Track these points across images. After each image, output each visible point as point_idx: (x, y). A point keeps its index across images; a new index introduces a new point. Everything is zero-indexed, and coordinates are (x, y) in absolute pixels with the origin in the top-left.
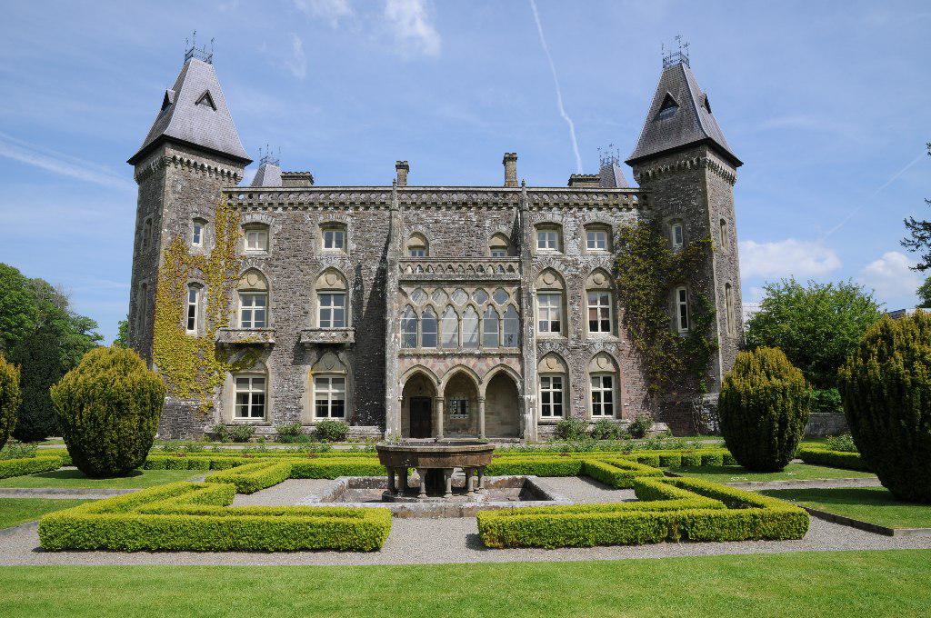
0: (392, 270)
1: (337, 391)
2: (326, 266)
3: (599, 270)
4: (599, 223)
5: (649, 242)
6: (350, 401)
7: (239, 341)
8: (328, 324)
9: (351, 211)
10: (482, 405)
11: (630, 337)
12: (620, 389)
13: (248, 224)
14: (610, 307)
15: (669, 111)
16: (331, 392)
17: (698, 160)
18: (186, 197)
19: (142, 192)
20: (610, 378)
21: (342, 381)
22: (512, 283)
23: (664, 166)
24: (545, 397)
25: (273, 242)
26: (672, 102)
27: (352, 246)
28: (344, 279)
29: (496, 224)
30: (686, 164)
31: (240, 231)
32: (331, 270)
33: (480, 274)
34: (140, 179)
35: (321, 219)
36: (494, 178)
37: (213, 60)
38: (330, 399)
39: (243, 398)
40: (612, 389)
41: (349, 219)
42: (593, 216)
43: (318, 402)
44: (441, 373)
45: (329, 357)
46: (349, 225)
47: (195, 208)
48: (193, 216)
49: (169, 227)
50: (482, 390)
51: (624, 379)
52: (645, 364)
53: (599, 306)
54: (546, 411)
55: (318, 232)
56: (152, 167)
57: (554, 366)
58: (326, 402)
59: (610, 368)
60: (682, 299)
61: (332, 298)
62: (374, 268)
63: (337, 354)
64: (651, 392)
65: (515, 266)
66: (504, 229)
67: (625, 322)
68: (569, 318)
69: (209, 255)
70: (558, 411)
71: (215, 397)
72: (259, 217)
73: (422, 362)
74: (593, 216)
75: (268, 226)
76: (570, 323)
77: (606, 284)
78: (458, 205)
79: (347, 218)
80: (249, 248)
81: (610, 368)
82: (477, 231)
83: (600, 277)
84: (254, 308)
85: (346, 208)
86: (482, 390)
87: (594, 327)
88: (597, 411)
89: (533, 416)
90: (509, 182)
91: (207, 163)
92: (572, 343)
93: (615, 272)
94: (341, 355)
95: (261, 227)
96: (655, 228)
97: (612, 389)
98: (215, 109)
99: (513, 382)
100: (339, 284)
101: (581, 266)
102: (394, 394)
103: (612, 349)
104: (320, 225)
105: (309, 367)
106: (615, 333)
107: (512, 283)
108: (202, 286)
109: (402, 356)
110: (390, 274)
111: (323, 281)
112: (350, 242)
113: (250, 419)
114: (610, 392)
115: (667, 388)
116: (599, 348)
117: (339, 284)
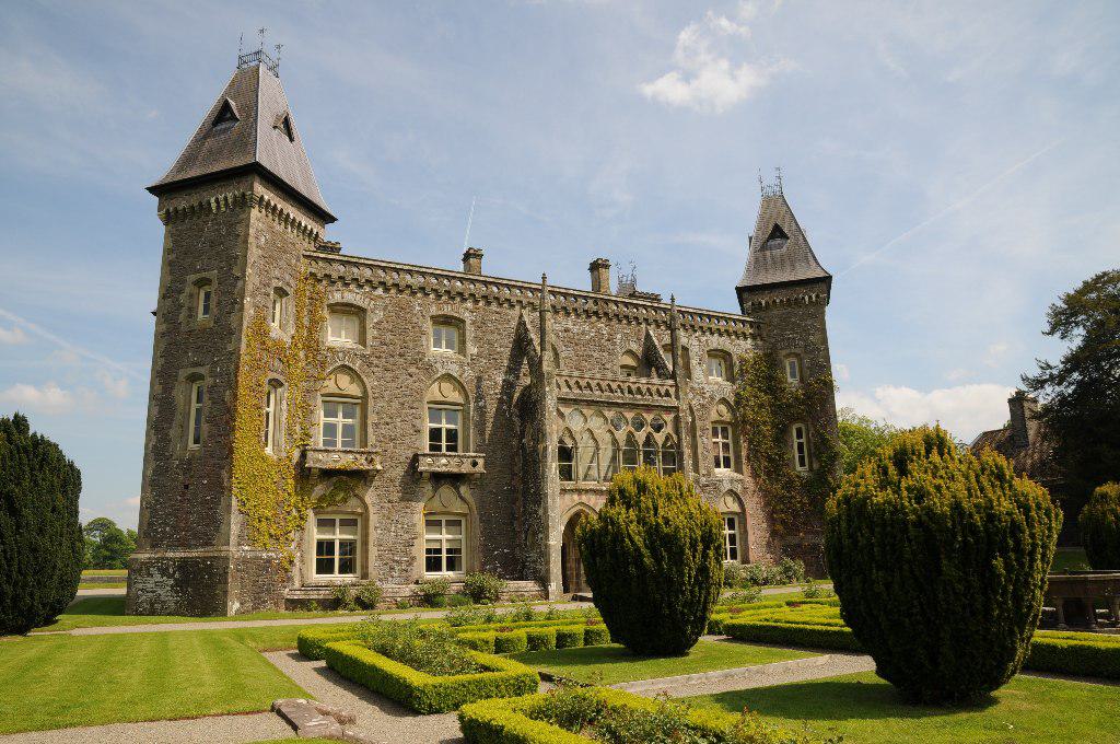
0: (549, 384)
1: (450, 537)
2: (442, 372)
3: (724, 401)
4: (722, 351)
5: (766, 375)
6: (471, 549)
7: (331, 465)
8: (439, 448)
9: (469, 304)
11: (755, 475)
12: (746, 532)
13: (337, 304)
14: (730, 441)
15: (779, 241)
16: (444, 538)
17: (817, 296)
18: (274, 253)
19: (169, 234)
20: (733, 519)
21: (458, 523)
22: (668, 409)
23: (779, 297)
25: (371, 333)
26: (777, 233)
27: (472, 349)
28: (462, 388)
29: (626, 342)
30: (803, 298)
31: (326, 313)
32: (448, 377)
33: (639, 397)
34: (169, 218)
35: (434, 310)
36: (584, 283)
37: (280, 71)
38: (445, 547)
39: (325, 548)
40: (735, 532)
41: (467, 314)
42: (716, 342)
43: (428, 551)
45: (446, 491)
46: (468, 322)
47: (277, 273)
48: (275, 283)
49: (253, 296)
51: (750, 522)
52: (767, 504)
53: (720, 440)
55: (428, 326)
56: (214, 205)
58: (439, 551)
59: (735, 508)
60: (799, 436)
61: (443, 413)
62: (500, 379)
63: (457, 489)
64: (774, 533)
65: (672, 391)
66: (634, 347)
67: (748, 458)
68: (699, 451)
69: (287, 340)
71: (293, 546)
72: (352, 296)
73: (584, 498)
74: (716, 342)
75: (363, 310)
76: (700, 457)
77: (727, 417)
79: (465, 311)
80: (338, 336)
81: (735, 508)
82: (604, 345)
83: (723, 408)
85: (464, 300)
87: (718, 465)
90: (597, 284)
91: (293, 212)
92: (703, 480)
93: (737, 403)
94: (463, 490)
95: (356, 312)
96: (770, 360)
97: (735, 532)
98: (292, 140)
100: (455, 397)
101: (707, 395)
103: (738, 488)
104: (432, 317)
105: (422, 504)
106: (738, 470)
107: (668, 409)
108: (282, 385)
109: (564, 491)
110: (547, 389)
111: (434, 392)
112: (469, 344)
113: (337, 578)
114: (734, 535)
115: (792, 529)
116: (727, 486)
117: (455, 397)
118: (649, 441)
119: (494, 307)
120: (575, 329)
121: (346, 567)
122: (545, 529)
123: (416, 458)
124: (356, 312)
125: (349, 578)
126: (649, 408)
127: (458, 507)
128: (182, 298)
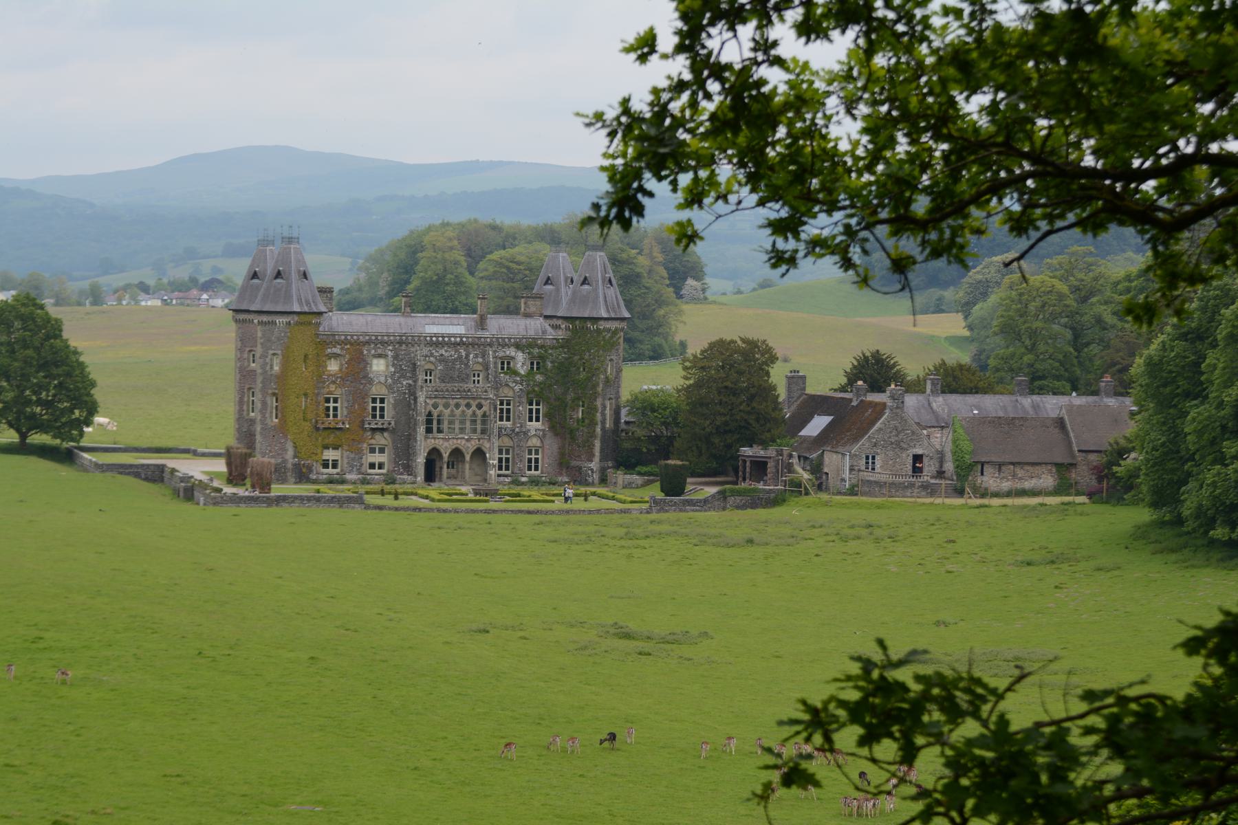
10: (467, 466)
24: (500, 460)
44: (446, 448)
45: (378, 436)
50: (468, 458)
54: (500, 468)
57: (507, 442)
70: (507, 469)
72: (337, 350)
78: (456, 344)
84: (331, 405)
86: (468, 458)
87: (531, 420)
88: (530, 469)
89: (493, 473)
94: (386, 434)
95: (336, 356)
99: (484, 454)
102: (421, 460)
118: (474, 414)
119: (404, 347)
120: (446, 354)
121: (335, 466)
122: (415, 454)
123: (363, 422)
124: (336, 356)
125: (335, 471)
126: (474, 398)
127: (383, 442)
128: (268, 360)
